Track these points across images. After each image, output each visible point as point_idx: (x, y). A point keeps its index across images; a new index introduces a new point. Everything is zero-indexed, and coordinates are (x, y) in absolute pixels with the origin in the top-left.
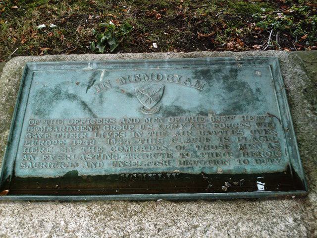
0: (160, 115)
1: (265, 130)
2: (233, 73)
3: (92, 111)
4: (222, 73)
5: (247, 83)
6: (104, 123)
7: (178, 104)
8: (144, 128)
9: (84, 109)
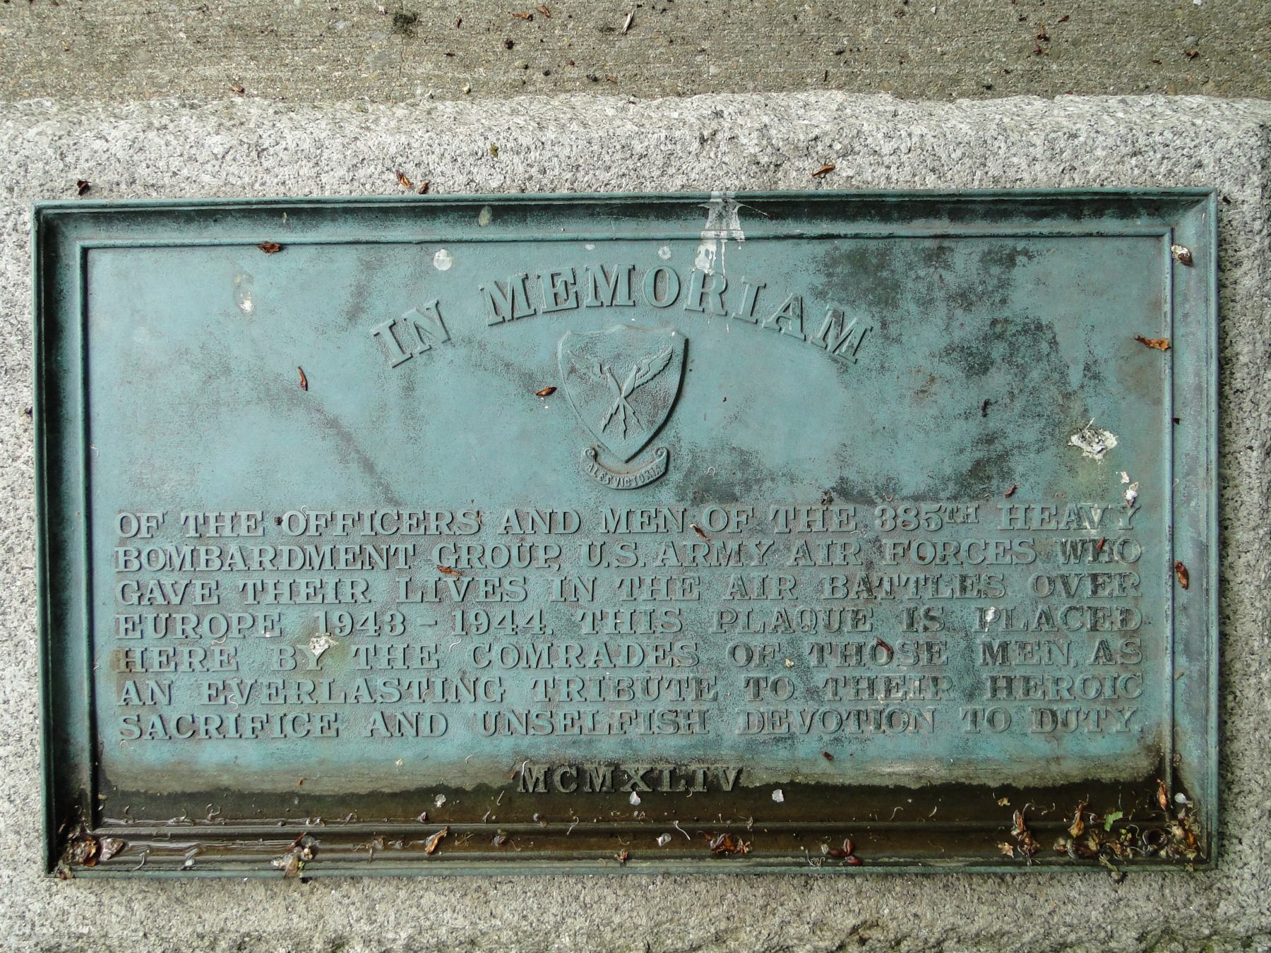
0: (666, 496)
1: (1094, 577)
2: (995, 270)
3: (379, 469)
4: (947, 267)
5: (1050, 327)
6: (432, 530)
7: (743, 439)
8: (598, 554)
9: (344, 460)
